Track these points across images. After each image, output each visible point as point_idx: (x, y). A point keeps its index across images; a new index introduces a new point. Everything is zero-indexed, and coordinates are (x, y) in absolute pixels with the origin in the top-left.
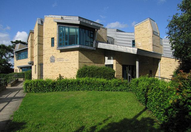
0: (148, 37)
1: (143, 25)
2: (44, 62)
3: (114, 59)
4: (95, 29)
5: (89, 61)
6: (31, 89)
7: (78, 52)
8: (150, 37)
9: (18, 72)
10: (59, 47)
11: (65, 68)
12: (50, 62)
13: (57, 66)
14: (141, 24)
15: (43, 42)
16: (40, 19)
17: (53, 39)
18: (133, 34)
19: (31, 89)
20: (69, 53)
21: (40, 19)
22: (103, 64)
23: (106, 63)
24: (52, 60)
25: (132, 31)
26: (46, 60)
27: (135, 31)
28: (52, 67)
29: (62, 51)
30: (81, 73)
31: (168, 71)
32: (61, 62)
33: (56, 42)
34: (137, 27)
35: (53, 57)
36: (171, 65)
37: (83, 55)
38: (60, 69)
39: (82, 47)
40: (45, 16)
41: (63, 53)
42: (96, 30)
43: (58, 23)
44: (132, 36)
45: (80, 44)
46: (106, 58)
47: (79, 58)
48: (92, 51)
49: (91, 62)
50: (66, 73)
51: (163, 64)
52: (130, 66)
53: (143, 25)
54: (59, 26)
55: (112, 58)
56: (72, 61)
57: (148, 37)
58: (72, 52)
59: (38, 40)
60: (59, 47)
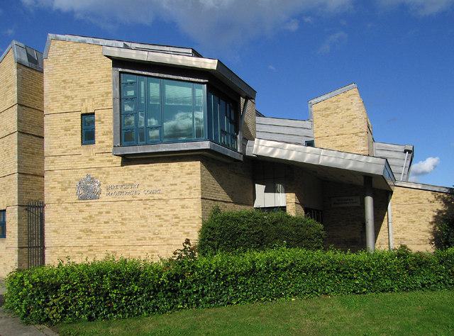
0: (356, 134)
1: (337, 101)
2: (50, 196)
3: (286, 191)
4: (239, 96)
5: (223, 195)
6: (66, 305)
7: (198, 164)
8: (361, 134)
9: (293, 214)
10: (121, 145)
11: (143, 217)
12: (75, 198)
13: (108, 212)
14: (334, 99)
15: (42, 127)
16: (23, 45)
17: (88, 121)
18: (307, 124)
19: (66, 305)
20: (160, 166)
21: (23, 45)
22: (249, 205)
23: (259, 203)
24: (88, 192)
25: (307, 116)
26: (54, 191)
27: (315, 115)
28: (86, 214)
29: (127, 160)
30: (218, 233)
31: (413, 222)
32: (129, 197)
33: (105, 129)
34: (318, 106)
35: (92, 180)
36: (422, 207)
37: (211, 178)
38: (123, 224)
39: (216, 150)
40: (51, 36)
41: (137, 166)
42: (242, 100)
43: (117, 62)
44: (304, 130)
45: (210, 138)
46: (260, 188)
47: (202, 186)
48: (227, 164)
49: (228, 199)
50: (150, 235)
51: (398, 204)
52: (317, 210)
53: (337, 101)
54: (120, 72)
55: (280, 187)
56: (174, 195)
57: (356, 134)
58: (174, 166)
59: (19, 121)
60: (121, 145)
